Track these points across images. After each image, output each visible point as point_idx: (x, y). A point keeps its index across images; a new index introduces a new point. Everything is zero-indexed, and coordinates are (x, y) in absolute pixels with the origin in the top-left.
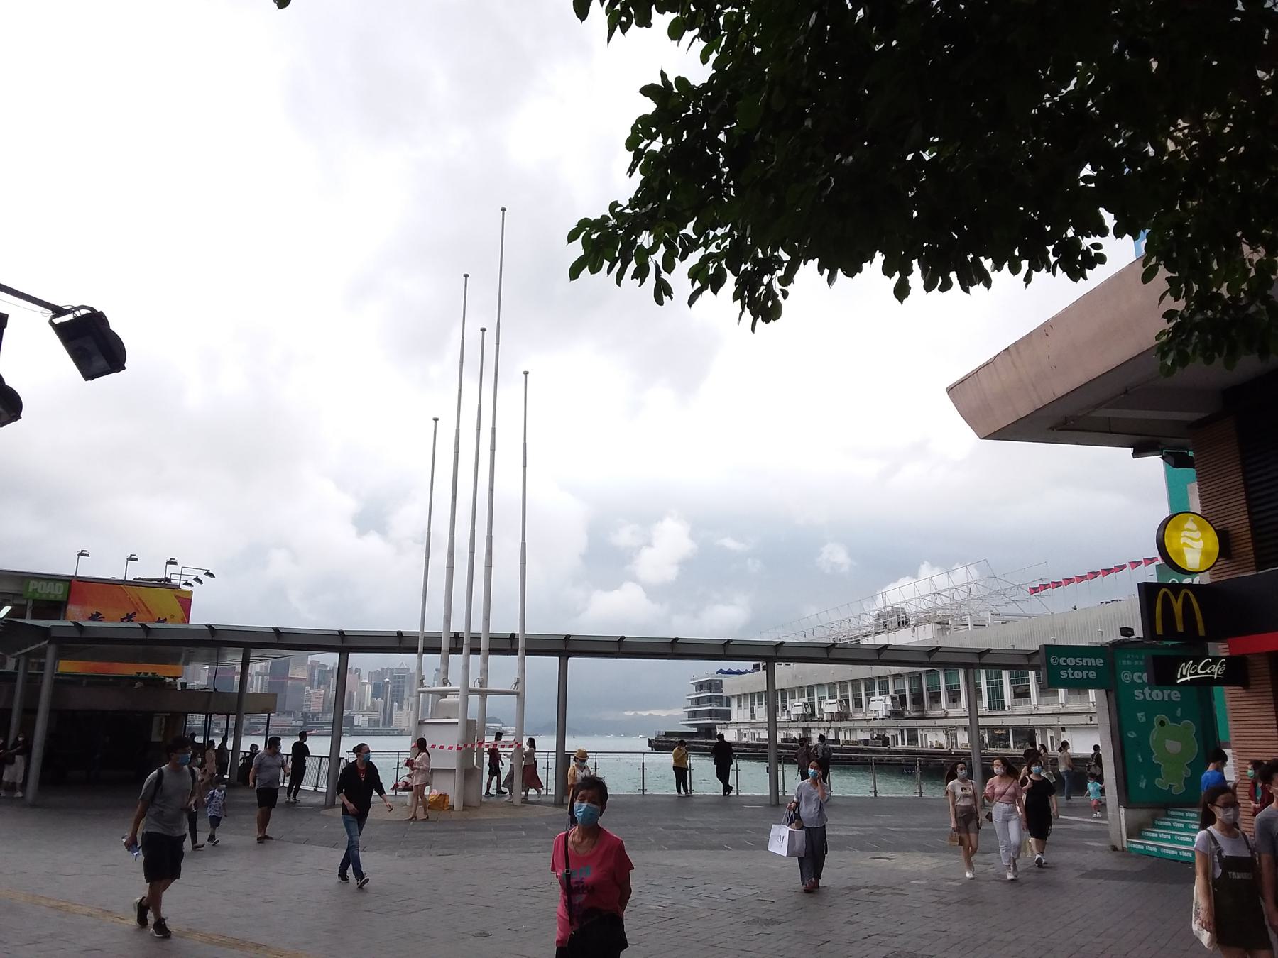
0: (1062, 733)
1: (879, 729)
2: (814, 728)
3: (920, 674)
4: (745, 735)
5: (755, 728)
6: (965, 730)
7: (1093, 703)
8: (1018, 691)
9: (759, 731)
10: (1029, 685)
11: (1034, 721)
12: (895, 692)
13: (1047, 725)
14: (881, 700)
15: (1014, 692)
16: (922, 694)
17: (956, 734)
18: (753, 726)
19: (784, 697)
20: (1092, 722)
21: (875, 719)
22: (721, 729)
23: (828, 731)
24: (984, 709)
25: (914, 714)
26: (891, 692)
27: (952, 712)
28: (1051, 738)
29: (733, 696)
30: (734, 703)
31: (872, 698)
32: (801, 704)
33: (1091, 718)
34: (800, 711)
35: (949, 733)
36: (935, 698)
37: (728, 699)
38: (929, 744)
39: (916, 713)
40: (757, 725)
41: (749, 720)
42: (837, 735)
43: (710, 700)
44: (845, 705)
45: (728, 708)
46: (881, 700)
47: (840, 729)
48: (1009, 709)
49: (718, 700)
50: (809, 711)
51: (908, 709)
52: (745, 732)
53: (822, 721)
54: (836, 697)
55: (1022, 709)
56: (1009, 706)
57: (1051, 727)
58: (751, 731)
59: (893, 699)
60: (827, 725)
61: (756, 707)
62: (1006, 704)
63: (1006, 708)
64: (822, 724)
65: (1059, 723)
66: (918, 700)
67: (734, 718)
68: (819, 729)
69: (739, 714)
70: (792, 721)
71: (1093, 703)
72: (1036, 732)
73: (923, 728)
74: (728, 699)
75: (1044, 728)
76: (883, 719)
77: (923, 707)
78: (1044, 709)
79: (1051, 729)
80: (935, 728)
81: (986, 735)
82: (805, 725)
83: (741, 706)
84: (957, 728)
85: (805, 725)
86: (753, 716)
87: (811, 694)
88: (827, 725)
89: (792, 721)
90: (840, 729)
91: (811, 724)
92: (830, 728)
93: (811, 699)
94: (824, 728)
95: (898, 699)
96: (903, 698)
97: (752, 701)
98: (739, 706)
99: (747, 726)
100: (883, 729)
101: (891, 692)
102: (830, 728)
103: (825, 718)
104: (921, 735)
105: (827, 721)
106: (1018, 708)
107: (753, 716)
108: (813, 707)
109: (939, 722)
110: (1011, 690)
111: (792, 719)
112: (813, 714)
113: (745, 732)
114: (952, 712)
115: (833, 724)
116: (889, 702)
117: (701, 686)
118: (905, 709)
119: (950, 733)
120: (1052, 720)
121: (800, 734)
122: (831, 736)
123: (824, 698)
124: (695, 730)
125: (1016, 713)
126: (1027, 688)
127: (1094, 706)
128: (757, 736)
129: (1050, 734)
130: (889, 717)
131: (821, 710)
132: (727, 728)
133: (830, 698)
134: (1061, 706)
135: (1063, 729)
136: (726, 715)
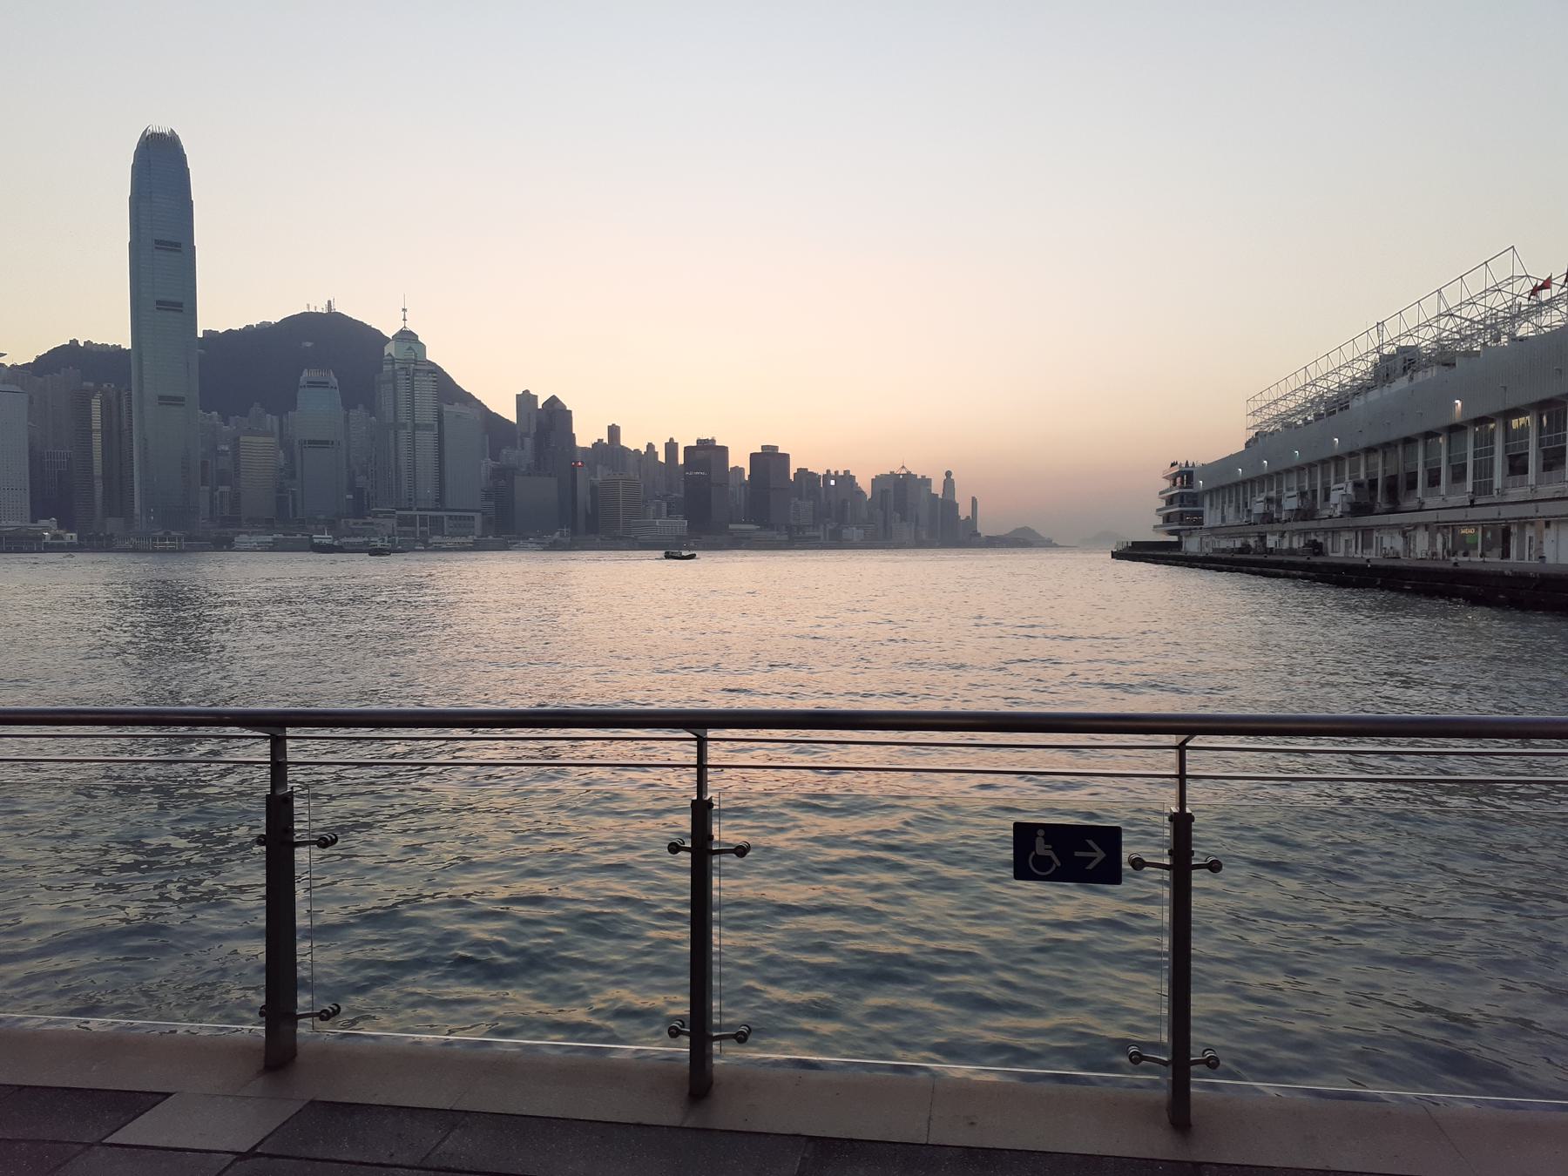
0: (1546, 531)
6: (1426, 530)
8: (1518, 463)
11: (1508, 512)
12: (1367, 475)
13: (1526, 518)
17: (1415, 537)
19: (1253, 492)
25: (1385, 506)
27: (1430, 502)
28: (1530, 538)
36: (1412, 484)
41: (1218, 523)
51: (1379, 501)
53: (1278, 522)
55: (1515, 494)
59: (1357, 485)
61: (1226, 506)
62: (1496, 486)
63: (1496, 492)
64: (1277, 527)
65: (1539, 514)
69: (1211, 518)
72: (1512, 530)
73: (1379, 527)
75: (1523, 522)
76: (1341, 517)
78: (1547, 491)
79: (1532, 524)
84: (1416, 526)
86: (1223, 519)
87: (1280, 485)
91: (1267, 527)
92: (1285, 532)
95: (1366, 486)
97: (1224, 498)
98: (1211, 505)
102: (1285, 532)
106: (1512, 491)
116: (1350, 491)
119: (1406, 532)
123: (1292, 489)
124: (1174, 539)
129: (1530, 532)
135: (1548, 524)
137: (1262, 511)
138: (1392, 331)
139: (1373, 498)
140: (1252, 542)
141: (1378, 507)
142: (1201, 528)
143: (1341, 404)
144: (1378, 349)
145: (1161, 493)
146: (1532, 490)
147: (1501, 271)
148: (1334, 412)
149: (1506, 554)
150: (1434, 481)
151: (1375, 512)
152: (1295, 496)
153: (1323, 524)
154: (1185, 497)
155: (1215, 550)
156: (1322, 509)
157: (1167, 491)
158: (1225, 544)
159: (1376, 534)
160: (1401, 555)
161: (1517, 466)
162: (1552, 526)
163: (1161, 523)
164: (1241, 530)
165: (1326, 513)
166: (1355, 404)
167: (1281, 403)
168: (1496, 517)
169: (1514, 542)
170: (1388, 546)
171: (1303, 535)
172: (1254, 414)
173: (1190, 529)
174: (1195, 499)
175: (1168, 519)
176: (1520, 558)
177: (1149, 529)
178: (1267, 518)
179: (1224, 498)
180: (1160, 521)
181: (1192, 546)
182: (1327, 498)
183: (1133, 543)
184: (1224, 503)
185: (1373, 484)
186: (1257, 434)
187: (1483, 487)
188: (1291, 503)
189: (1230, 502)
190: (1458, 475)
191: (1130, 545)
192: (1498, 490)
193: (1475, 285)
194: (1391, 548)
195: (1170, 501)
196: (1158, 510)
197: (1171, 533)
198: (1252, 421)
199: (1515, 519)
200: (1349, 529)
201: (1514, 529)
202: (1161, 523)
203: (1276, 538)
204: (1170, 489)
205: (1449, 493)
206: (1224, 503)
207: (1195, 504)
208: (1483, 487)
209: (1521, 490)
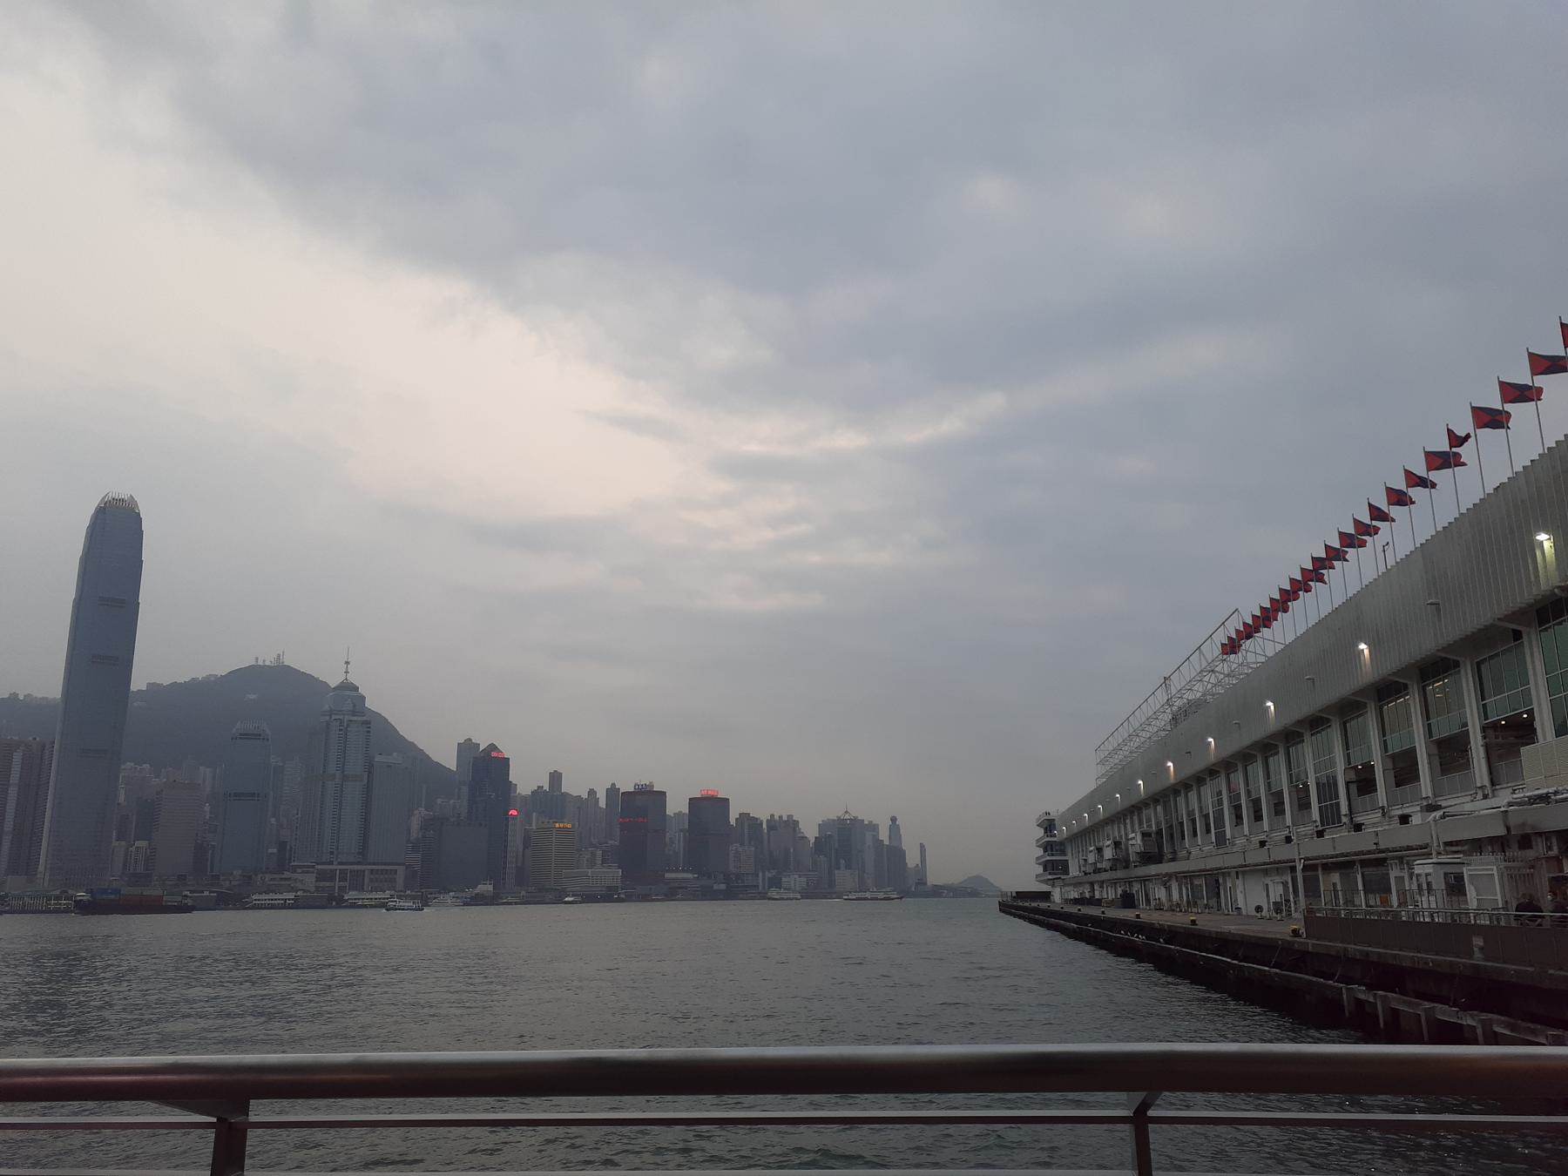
47: (1102, 883)
59: (1145, 835)
74: (1061, 843)
137: (1111, 857)
139: (1160, 847)
144: (1169, 703)
145: (1038, 841)
157: (1041, 838)
163: (1042, 872)
180: (1040, 870)
183: (1017, 892)
185: (1159, 832)
188: (1108, 853)
191: (1014, 894)
197: (1046, 882)
198: (1102, 770)
208: (1221, 840)
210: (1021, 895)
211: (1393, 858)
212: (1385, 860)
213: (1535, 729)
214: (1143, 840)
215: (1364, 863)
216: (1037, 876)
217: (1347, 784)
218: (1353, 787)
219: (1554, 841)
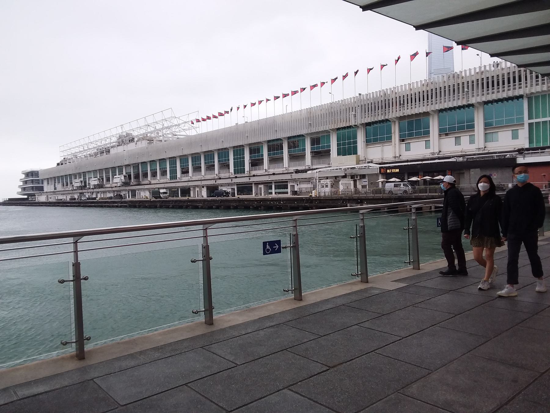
0: (202, 189)
1: (117, 191)
2: (86, 192)
3: (138, 164)
4: (51, 198)
5: (56, 194)
7: (216, 174)
8: (183, 170)
9: (58, 195)
10: (189, 168)
11: (190, 184)
12: (126, 173)
13: (196, 185)
14: (119, 177)
15: (182, 171)
16: (139, 174)
18: (54, 193)
19: (71, 179)
20: (216, 183)
21: (115, 187)
22: (38, 195)
23: (93, 194)
24: (168, 180)
26: (124, 173)
28: (198, 191)
29: (45, 179)
30: (45, 183)
31: (115, 177)
32: (79, 181)
33: (216, 181)
34: (79, 184)
35: (151, 191)
36: (145, 175)
37: (42, 181)
38: (141, 197)
39: (136, 183)
40: (56, 193)
41: (53, 190)
42: (97, 195)
43: (32, 181)
44: (101, 181)
45: (42, 185)
46: (119, 177)
47: (98, 192)
48: (179, 179)
49: (36, 181)
50: (83, 184)
51: (132, 181)
52: (50, 196)
53: (90, 189)
54: (97, 177)
56: (179, 178)
57: (198, 186)
58: (54, 196)
59: (125, 176)
60: (92, 191)
62: (178, 177)
63: (178, 179)
64: (89, 191)
65: (202, 184)
66: (137, 177)
67: (46, 190)
68: (88, 193)
69: (48, 188)
70: (75, 190)
71: (216, 174)
73: (139, 190)
74: (42, 181)
75: (195, 187)
76: (119, 186)
77: (139, 180)
78: (194, 178)
79: (198, 187)
80: (144, 190)
81: (168, 191)
82: (81, 191)
83: (49, 184)
85: (81, 191)
86: (55, 189)
88: (92, 191)
89: (75, 190)
90: (98, 192)
91: (84, 191)
92: (93, 192)
93: (85, 179)
94: (90, 192)
95: (127, 177)
96: (130, 176)
97: (55, 181)
98: (48, 184)
99: (51, 193)
100: (120, 191)
101: (124, 173)
102: (93, 192)
103: (91, 188)
104: (138, 193)
105: (92, 189)
106: (183, 178)
107: (55, 189)
108: (85, 182)
109: (146, 187)
110: (180, 170)
111: (74, 189)
112: (85, 186)
113: (50, 196)
114: (153, 182)
115: (95, 190)
116: (123, 178)
117: (28, 174)
118: (130, 181)
120: (198, 183)
121: (78, 196)
122: (94, 196)
123: (91, 178)
124: (26, 197)
125: (182, 181)
126: (187, 169)
127: (217, 176)
128: (56, 198)
129: (197, 189)
130: (123, 185)
131: (89, 184)
132: (41, 195)
133: (94, 178)
134: (202, 177)
136: (41, 189)
138: (127, 129)
140: (76, 197)
141: (132, 183)
142: (43, 192)
143: (106, 150)
146: (191, 178)
147: (167, 115)
148: (104, 152)
149: (190, 196)
150: (154, 175)
151: (131, 185)
152: (79, 182)
153: (107, 189)
154: (34, 181)
155: (57, 199)
156: (106, 184)
158: (60, 197)
159: (137, 192)
160: (149, 198)
161: (185, 172)
162: (204, 187)
163: (21, 191)
164: (71, 192)
165: (108, 185)
166: (112, 151)
167: (76, 148)
168: (187, 185)
169: (192, 193)
170: (144, 195)
171: (103, 193)
172: (63, 151)
173: (40, 193)
174: (38, 181)
175: (24, 189)
176: (193, 196)
177: (15, 193)
178: (81, 188)
179: (55, 181)
180: (20, 190)
181: (42, 198)
182: (108, 180)
184: (55, 183)
186: (64, 158)
187: (173, 176)
189: (59, 182)
190: (164, 173)
192: (179, 178)
193: (159, 117)
194: (145, 196)
195: (26, 182)
196: (20, 186)
199: (194, 186)
200: (125, 190)
201: (192, 189)
202: (21, 191)
203: (89, 194)
204: (25, 178)
205: (160, 179)
206: (55, 183)
207: (39, 183)
208: (173, 176)
209: (187, 178)
210: (10, 199)
211: (273, 182)
212: (288, 181)
213: (330, 154)
214: (124, 178)
215: (275, 182)
216: (18, 192)
217: (249, 163)
218: (250, 164)
219: (359, 176)
